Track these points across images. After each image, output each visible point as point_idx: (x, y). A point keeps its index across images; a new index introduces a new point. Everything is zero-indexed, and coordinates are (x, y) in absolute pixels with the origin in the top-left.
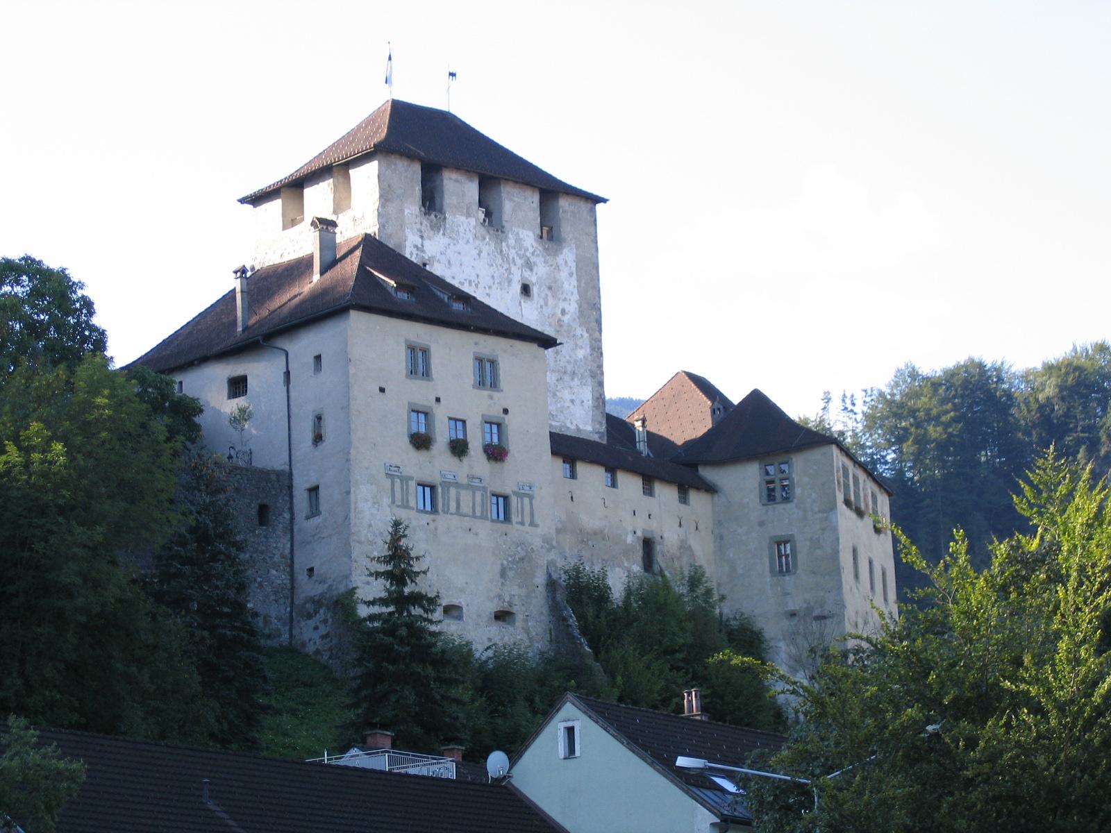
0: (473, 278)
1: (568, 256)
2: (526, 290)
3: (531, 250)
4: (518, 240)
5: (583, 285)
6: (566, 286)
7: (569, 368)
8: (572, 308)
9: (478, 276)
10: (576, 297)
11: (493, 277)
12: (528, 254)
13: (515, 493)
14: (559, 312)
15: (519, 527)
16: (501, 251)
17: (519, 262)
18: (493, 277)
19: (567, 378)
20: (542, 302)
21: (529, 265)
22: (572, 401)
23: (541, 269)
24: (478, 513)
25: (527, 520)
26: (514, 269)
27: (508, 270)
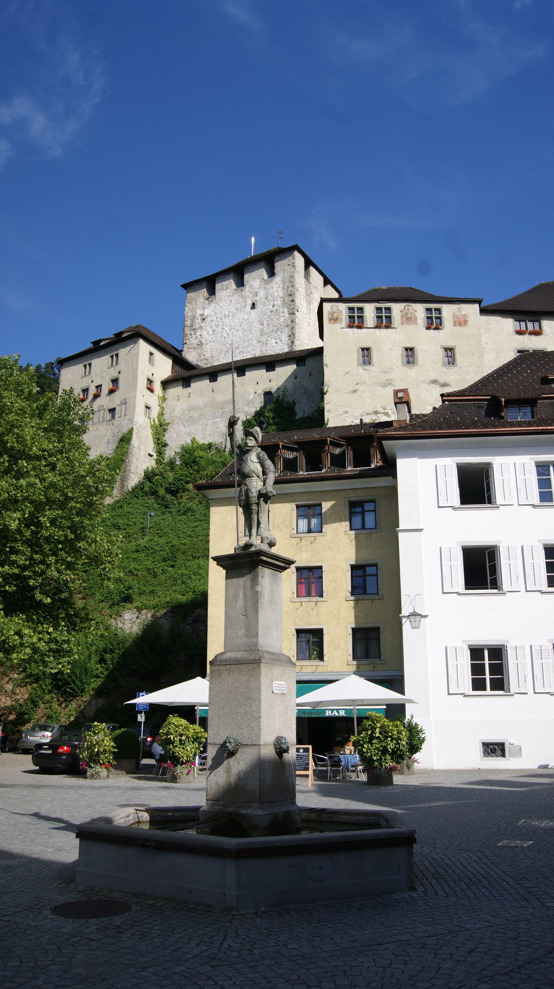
0: (227, 313)
1: (278, 279)
2: (253, 306)
3: (258, 287)
4: (251, 287)
5: (286, 288)
6: (276, 293)
7: (275, 328)
8: (279, 302)
9: (229, 312)
10: (281, 294)
11: (237, 309)
12: (256, 290)
13: (119, 405)
14: (271, 307)
15: (119, 419)
16: (242, 295)
17: (251, 295)
18: (237, 309)
19: (274, 333)
20: (262, 306)
21: (256, 294)
22: (276, 343)
23: (262, 293)
24: (101, 421)
25: (123, 414)
26: (247, 299)
27: (246, 302)
